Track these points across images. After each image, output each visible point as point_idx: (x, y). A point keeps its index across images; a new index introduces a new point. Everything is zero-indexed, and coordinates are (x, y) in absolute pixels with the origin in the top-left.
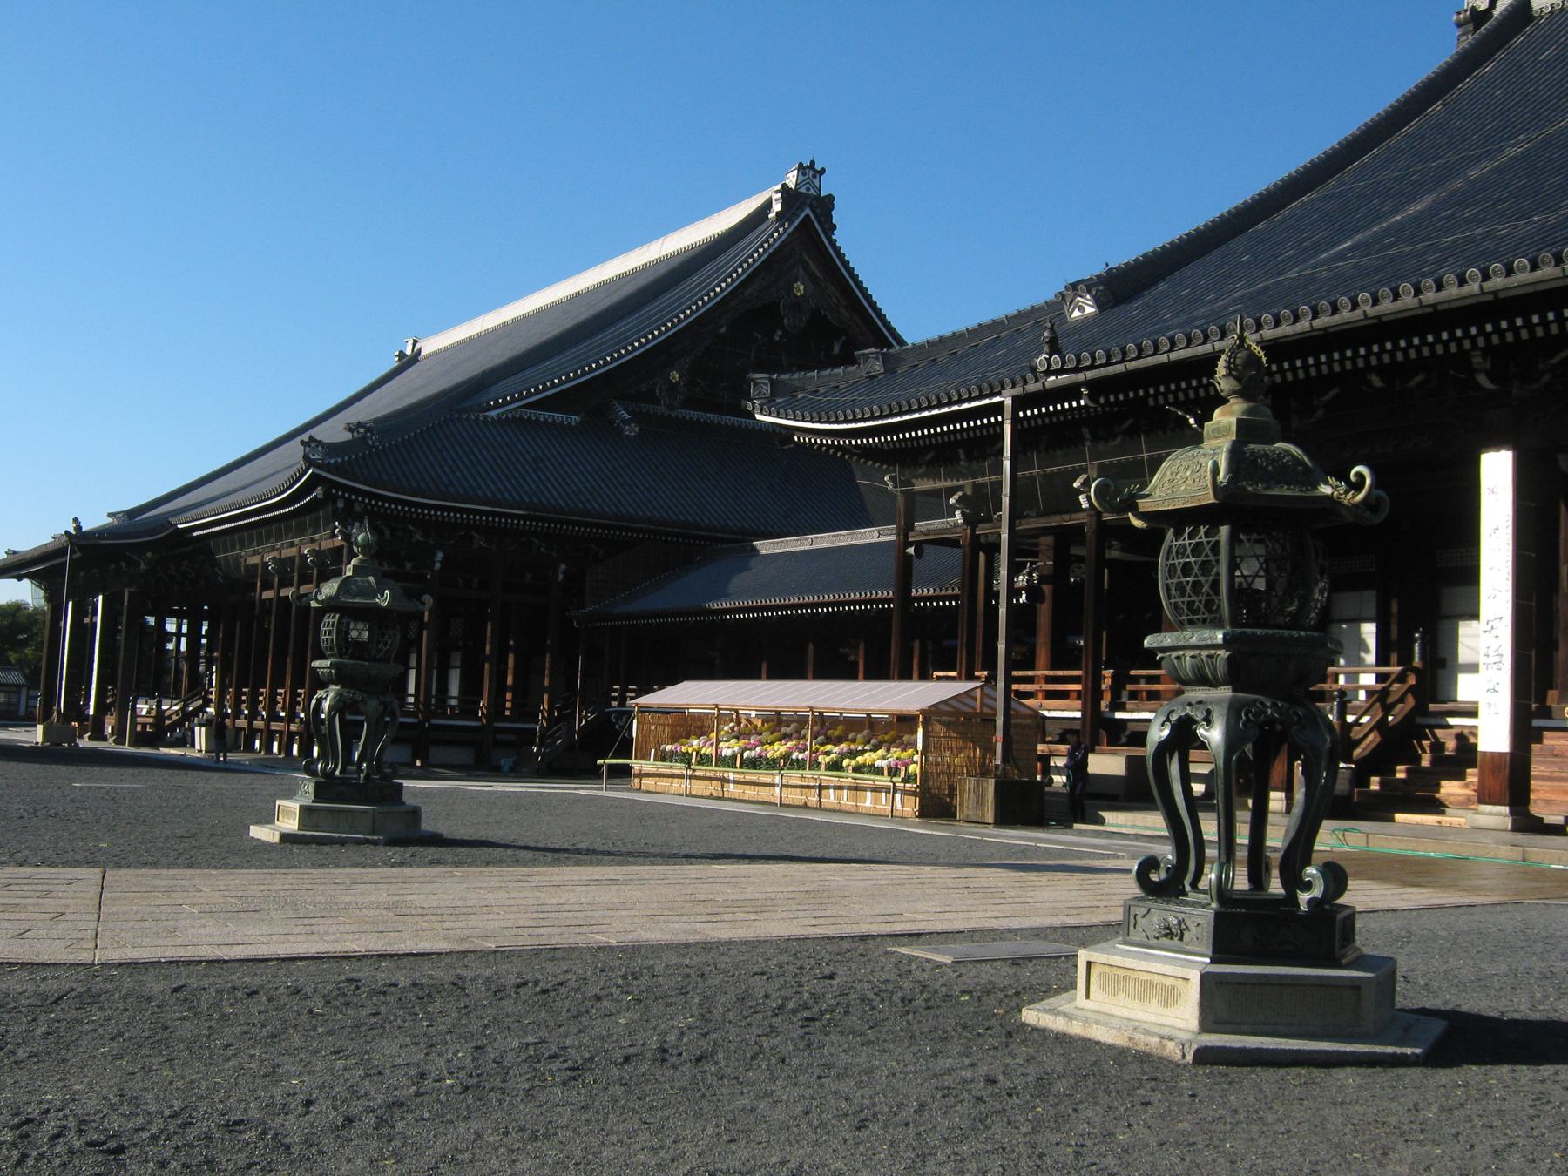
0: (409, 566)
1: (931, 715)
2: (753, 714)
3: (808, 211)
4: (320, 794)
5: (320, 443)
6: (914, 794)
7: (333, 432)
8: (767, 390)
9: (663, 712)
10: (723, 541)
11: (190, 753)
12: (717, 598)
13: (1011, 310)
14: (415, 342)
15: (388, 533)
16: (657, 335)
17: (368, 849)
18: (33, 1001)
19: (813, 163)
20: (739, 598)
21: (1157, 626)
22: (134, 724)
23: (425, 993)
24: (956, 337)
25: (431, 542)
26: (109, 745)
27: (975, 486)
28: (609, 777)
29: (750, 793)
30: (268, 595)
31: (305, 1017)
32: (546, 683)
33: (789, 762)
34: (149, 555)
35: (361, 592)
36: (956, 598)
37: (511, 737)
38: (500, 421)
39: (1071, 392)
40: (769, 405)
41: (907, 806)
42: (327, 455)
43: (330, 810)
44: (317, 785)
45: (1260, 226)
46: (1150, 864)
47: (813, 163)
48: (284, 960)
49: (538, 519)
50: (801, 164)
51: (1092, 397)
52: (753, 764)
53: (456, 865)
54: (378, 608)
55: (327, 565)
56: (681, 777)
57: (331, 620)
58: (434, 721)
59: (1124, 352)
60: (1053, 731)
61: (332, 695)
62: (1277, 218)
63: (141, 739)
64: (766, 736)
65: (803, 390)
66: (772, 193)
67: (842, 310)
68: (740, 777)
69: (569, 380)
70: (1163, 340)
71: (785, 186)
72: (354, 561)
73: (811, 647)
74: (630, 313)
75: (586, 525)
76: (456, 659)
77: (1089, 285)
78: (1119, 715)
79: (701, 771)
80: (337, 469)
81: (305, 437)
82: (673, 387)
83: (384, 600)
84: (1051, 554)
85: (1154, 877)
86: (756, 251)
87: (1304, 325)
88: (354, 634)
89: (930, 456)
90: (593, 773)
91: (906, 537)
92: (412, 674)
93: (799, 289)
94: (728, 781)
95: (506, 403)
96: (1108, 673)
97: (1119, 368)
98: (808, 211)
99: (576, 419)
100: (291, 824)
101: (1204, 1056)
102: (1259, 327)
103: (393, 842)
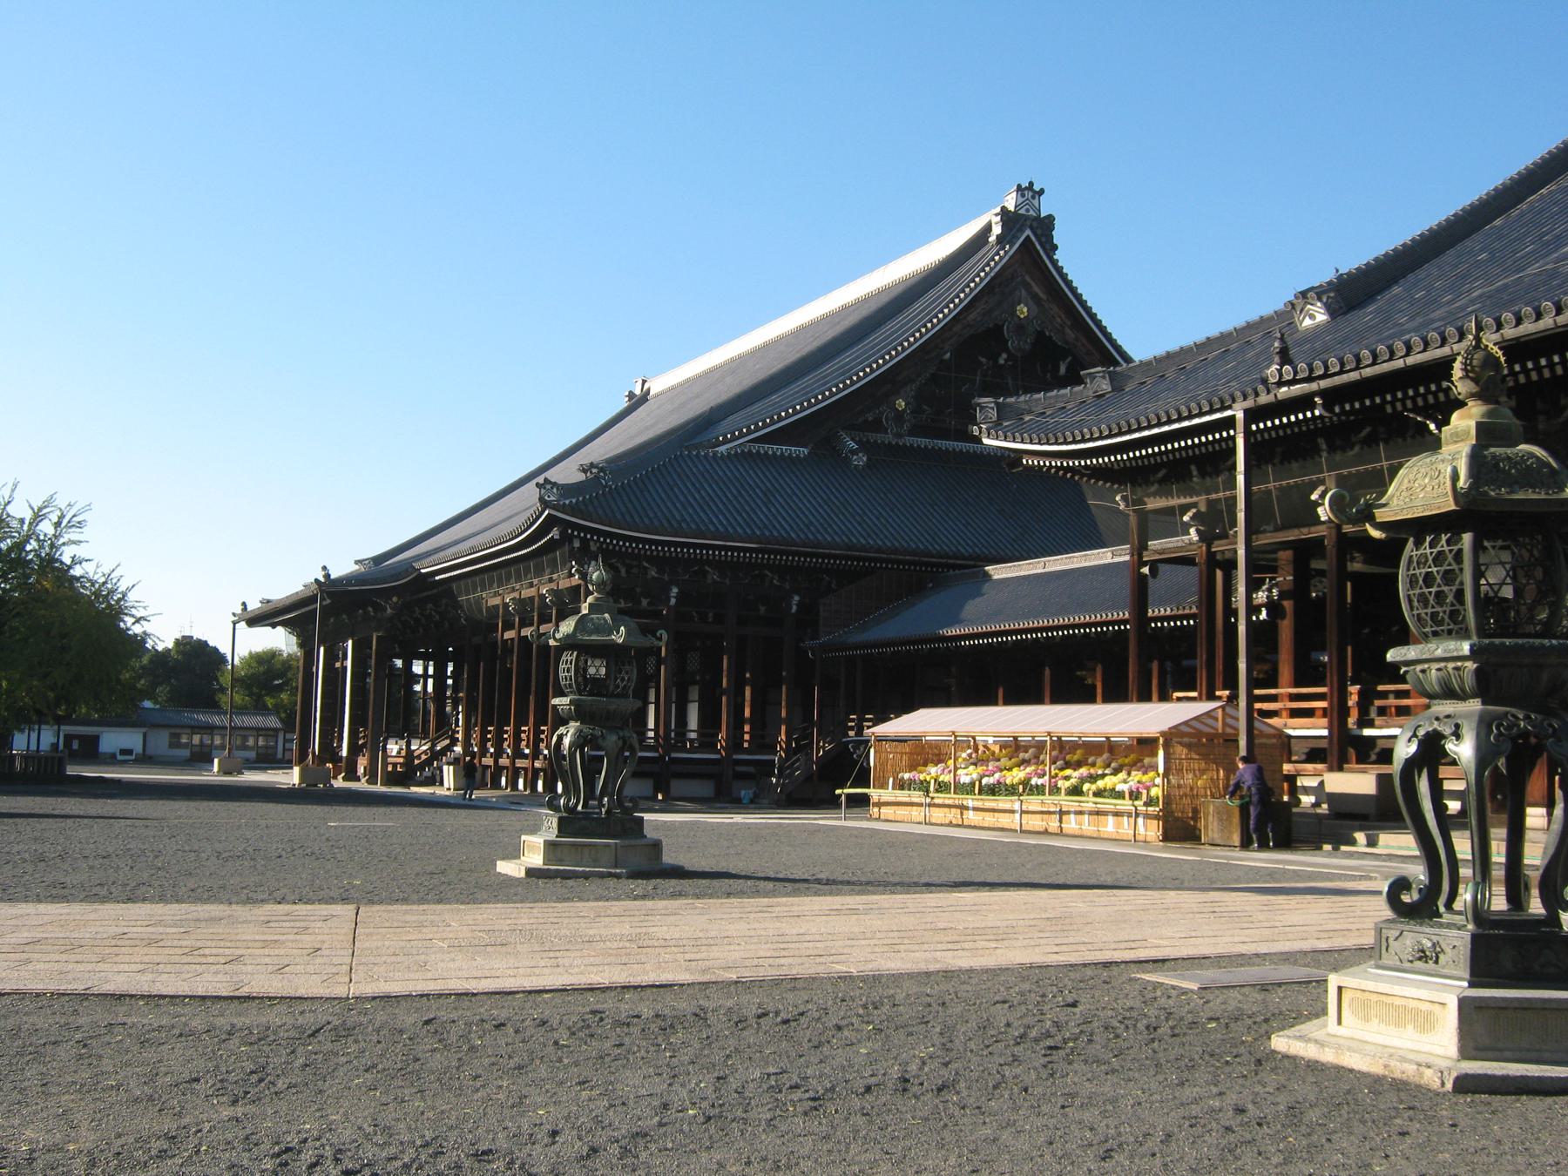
0: (645, 602)
1: (1172, 736)
2: (991, 740)
3: (1029, 233)
4: (564, 827)
5: (554, 484)
6: (1157, 817)
7: (568, 474)
8: (994, 415)
9: (901, 740)
10: (954, 567)
11: (440, 791)
12: (950, 625)
13: (1239, 322)
14: (644, 382)
15: (623, 571)
16: (883, 364)
17: (611, 882)
18: (293, 1034)
19: (1031, 184)
20: (974, 622)
21: (1404, 638)
22: (385, 764)
23: (668, 1025)
24: (1184, 352)
25: (666, 577)
26: (362, 785)
27: (1210, 503)
28: (847, 807)
29: (990, 820)
30: (509, 635)
31: (551, 1049)
32: (784, 714)
33: (1028, 788)
34: (395, 599)
35: (597, 631)
36: (1193, 616)
37: (751, 769)
38: (729, 456)
39: (1304, 402)
40: (996, 428)
41: (1151, 831)
42: (563, 496)
43: (573, 845)
44: (561, 820)
45: (1498, 222)
46: (1400, 885)
47: (1031, 184)
48: (530, 992)
49: (770, 552)
50: (1019, 186)
51: (1327, 406)
52: (992, 790)
53: (697, 897)
54: (614, 645)
55: (565, 604)
56: (921, 805)
57: (569, 658)
58: (674, 755)
59: (1358, 360)
60: (1299, 750)
61: (572, 731)
62: (1514, 213)
63: (392, 779)
64: (1004, 762)
65: (1030, 412)
66: (991, 217)
67: (1068, 331)
68: (979, 804)
69: (796, 412)
70: (1399, 346)
71: (1003, 208)
72: (590, 599)
73: (1047, 672)
75: (817, 555)
76: (694, 693)
77: (1319, 292)
78: (1367, 732)
79: (940, 798)
80: (572, 510)
81: (540, 479)
82: (899, 416)
83: (619, 637)
84: (1290, 568)
85: (1406, 898)
86: (977, 275)
87: (1547, 322)
88: (592, 671)
89: (1160, 474)
90: (832, 803)
91: (1140, 556)
92: (652, 708)
93: (1023, 311)
94: (967, 808)
95: (734, 439)
96: (1354, 689)
97: (1354, 376)
98: (1028, 232)
99: (804, 451)
100: (536, 859)
101: (1465, 1085)
102: (1499, 326)
103: (635, 875)
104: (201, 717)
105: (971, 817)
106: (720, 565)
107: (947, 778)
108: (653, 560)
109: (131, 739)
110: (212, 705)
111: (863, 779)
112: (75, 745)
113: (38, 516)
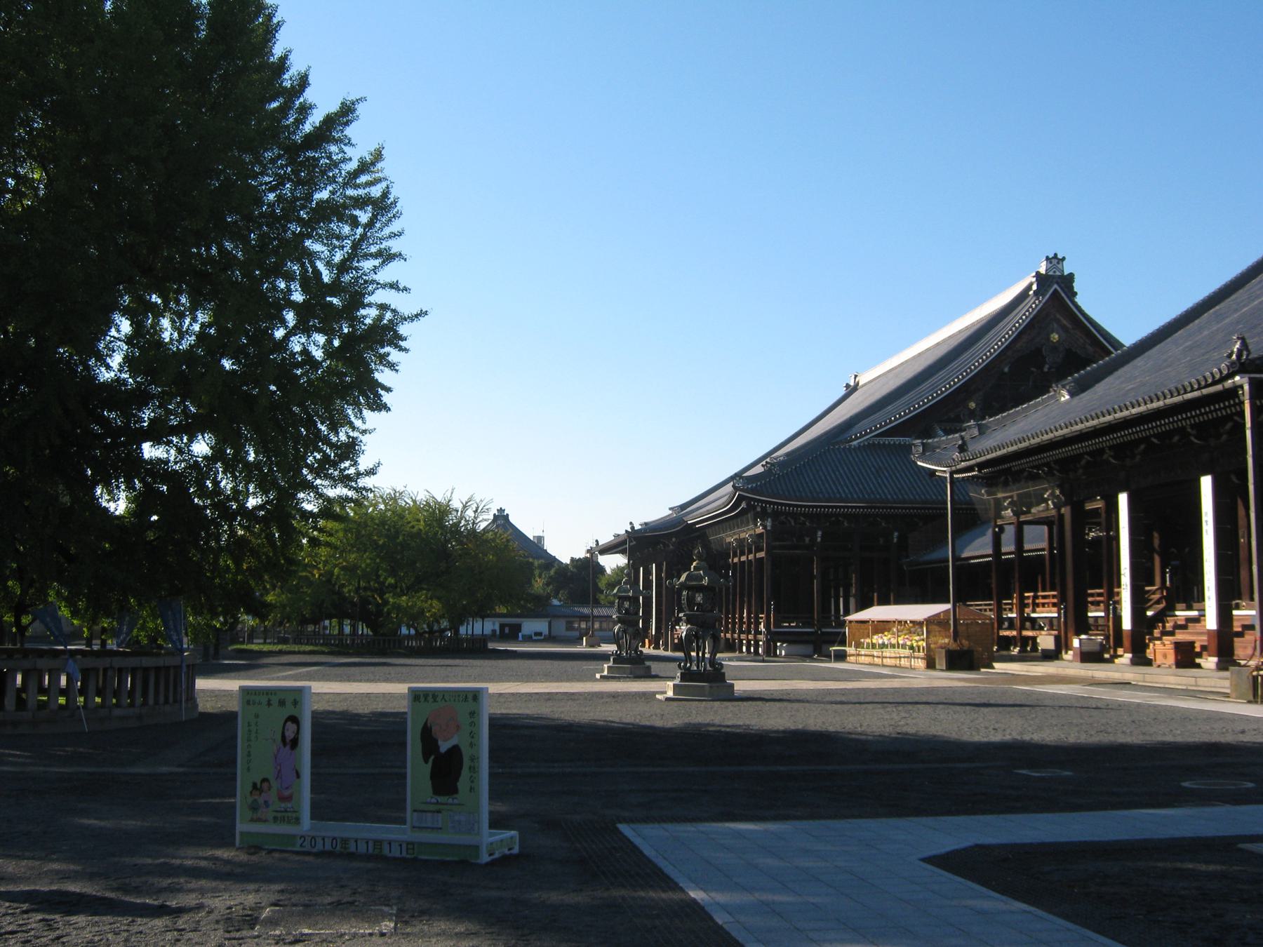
0: (807, 540)
1: (930, 621)
3: (1056, 288)
22: (673, 639)
30: (736, 560)
40: (923, 457)
41: (921, 664)
49: (875, 508)
50: (1047, 258)
51: (979, 471)
66: (1031, 278)
74: (941, 369)
75: (906, 508)
80: (752, 491)
93: (1055, 337)
95: (862, 436)
98: (1055, 286)
104: (586, 611)
105: (862, 659)
106: (845, 516)
107: (894, 641)
108: (804, 515)
109: (541, 626)
110: (597, 603)
111: (843, 643)
112: (507, 630)
113: (465, 507)
